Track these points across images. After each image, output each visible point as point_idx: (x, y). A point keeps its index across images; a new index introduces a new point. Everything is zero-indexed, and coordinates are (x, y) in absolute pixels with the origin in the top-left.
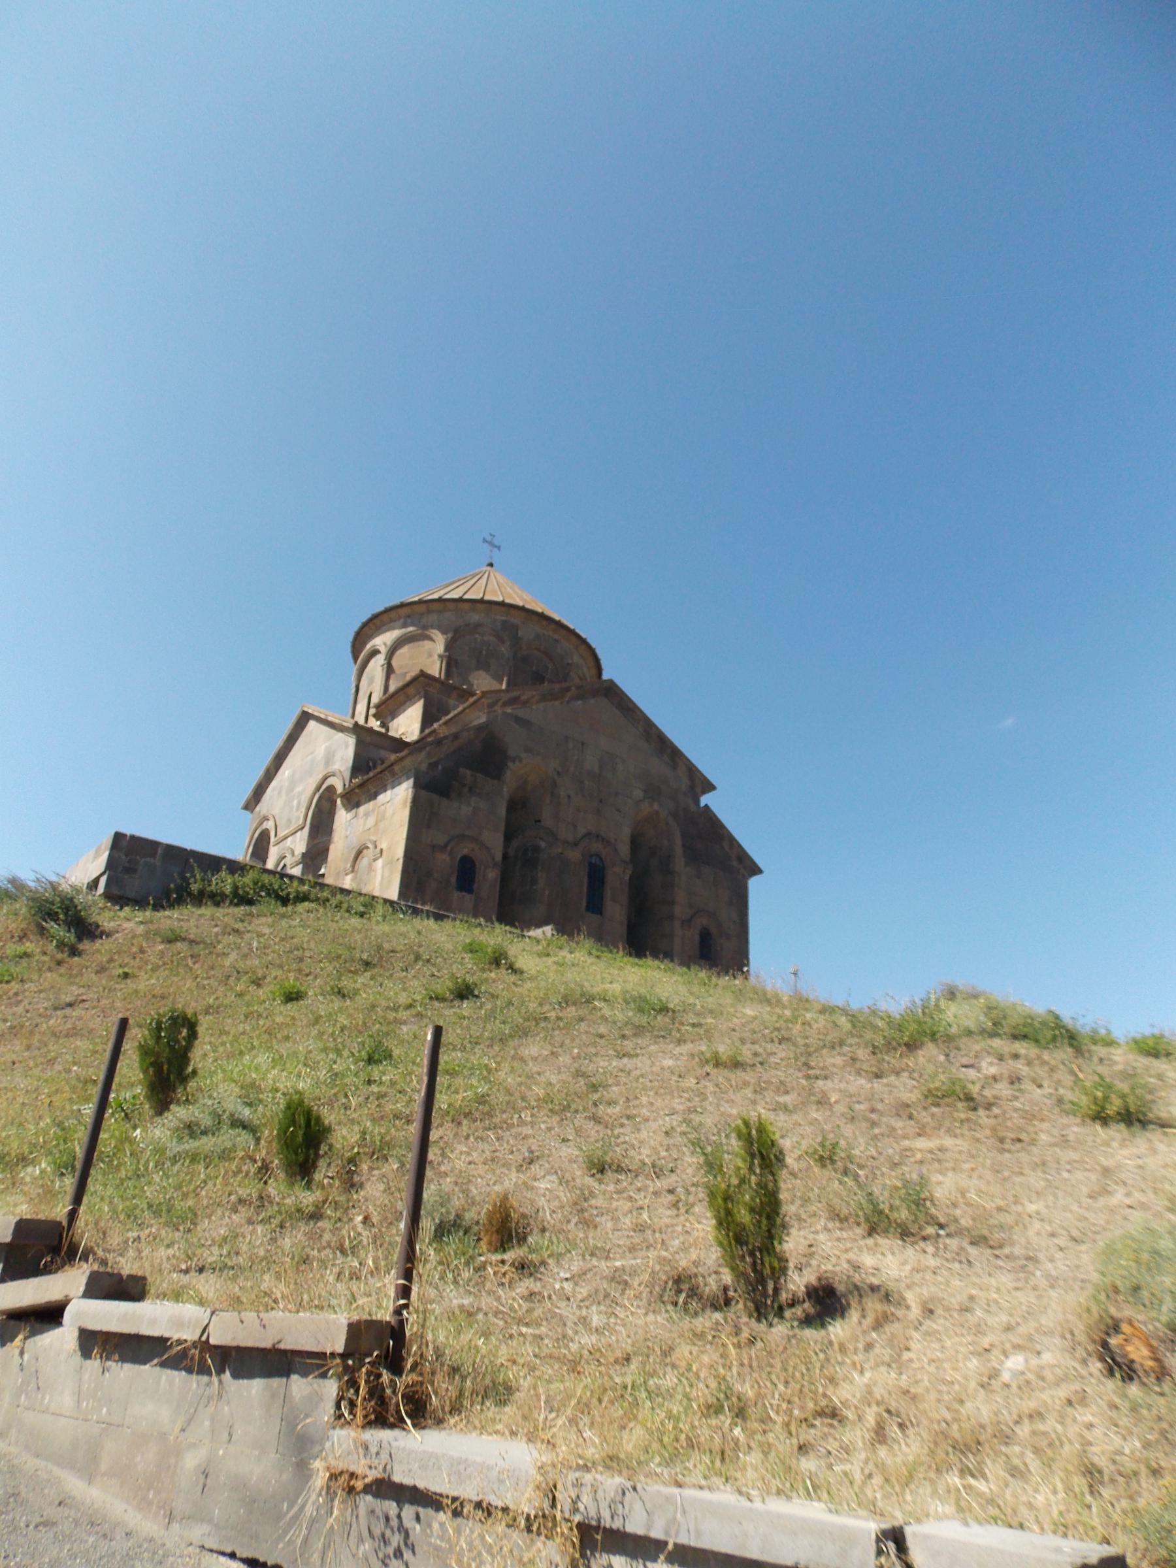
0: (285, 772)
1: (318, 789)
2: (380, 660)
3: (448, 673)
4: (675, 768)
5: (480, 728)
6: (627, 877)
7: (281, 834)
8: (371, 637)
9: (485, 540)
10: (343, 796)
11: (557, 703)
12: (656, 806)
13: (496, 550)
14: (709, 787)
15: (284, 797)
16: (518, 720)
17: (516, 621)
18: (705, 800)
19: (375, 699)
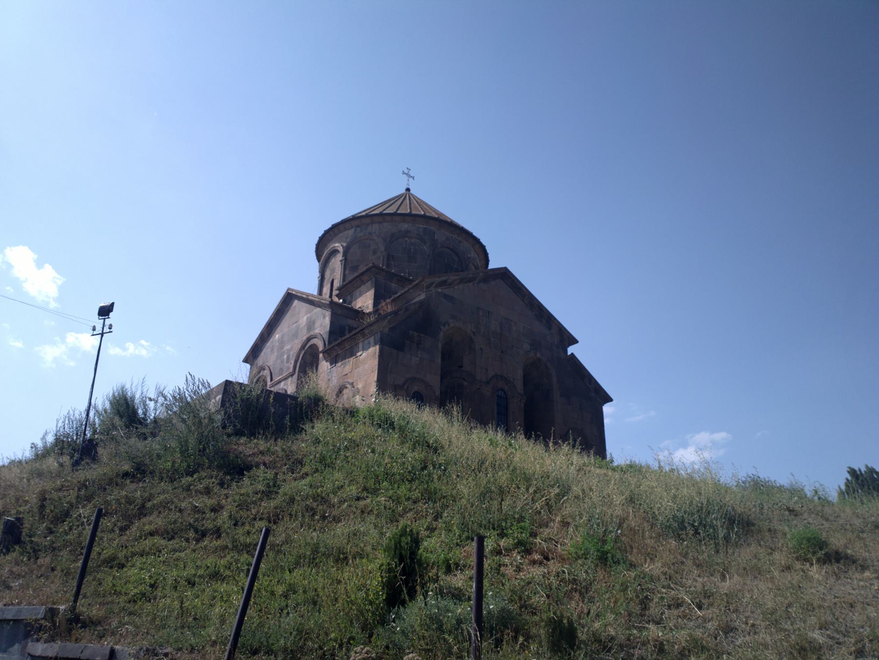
0: (277, 336)
1: (303, 347)
2: (340, 257)
3: (388, 265)
4: (550, 329)
5: (421, 303)
6: (523, 405)
7: (276, 379)
8: (330, 241)
9: (404, 173)
10: (324, 352)
11: (471, 284)
12: (538, 355)
13: (411, 179)
14: (574, 341)
15: (276, 354)
16: (446, 296)
17: (432, 228)
18: (571, 350)
19: (337, 284)
